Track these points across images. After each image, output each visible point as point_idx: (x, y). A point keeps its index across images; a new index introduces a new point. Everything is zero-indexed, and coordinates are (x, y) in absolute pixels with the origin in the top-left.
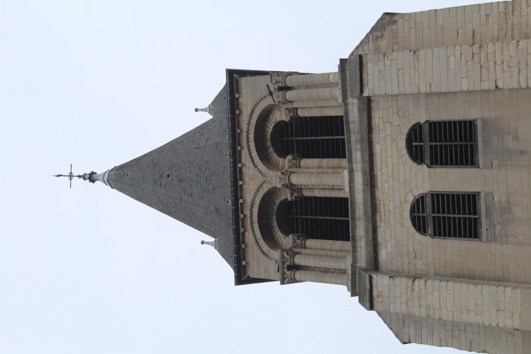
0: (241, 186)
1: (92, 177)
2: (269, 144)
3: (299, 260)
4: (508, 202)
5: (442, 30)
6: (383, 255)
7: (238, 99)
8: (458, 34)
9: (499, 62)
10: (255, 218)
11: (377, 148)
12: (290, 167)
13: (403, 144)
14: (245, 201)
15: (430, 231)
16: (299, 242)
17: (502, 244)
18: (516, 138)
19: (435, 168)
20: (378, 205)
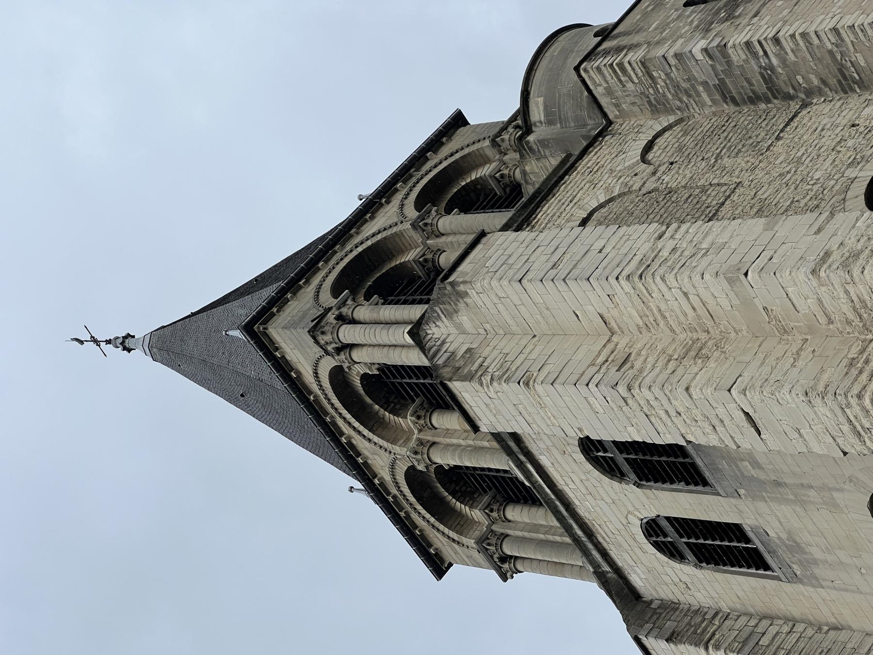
0: (366, 463)
1: (125, 343)
2: (368, 400)
3: (509, 549)
4: (790, 537)
5: (548, 309)
6: (637, 580)
7: (283, 357)
8: (577, 316)
9: (673, 413)
10: (412, 499)
11: (544, 460)
12: (420, 431)
13: (581, 457)
14: (382, 480)
15: (690, 556)
16: (495, 514)
17: (813, 586)
18: (756, 464)
19: (650, 488)
20: (591, 527)
